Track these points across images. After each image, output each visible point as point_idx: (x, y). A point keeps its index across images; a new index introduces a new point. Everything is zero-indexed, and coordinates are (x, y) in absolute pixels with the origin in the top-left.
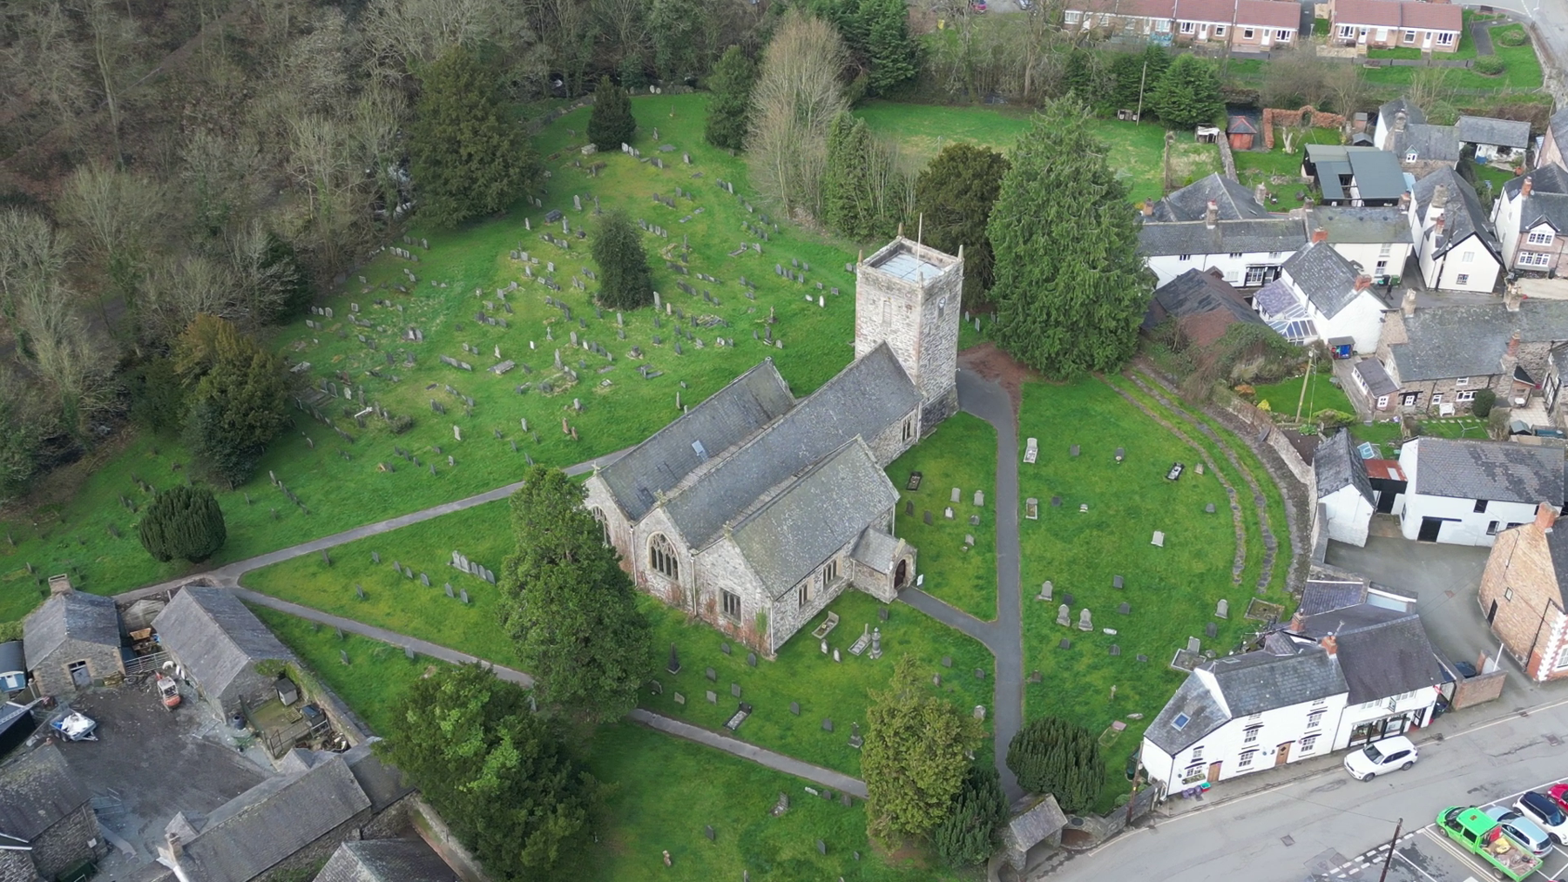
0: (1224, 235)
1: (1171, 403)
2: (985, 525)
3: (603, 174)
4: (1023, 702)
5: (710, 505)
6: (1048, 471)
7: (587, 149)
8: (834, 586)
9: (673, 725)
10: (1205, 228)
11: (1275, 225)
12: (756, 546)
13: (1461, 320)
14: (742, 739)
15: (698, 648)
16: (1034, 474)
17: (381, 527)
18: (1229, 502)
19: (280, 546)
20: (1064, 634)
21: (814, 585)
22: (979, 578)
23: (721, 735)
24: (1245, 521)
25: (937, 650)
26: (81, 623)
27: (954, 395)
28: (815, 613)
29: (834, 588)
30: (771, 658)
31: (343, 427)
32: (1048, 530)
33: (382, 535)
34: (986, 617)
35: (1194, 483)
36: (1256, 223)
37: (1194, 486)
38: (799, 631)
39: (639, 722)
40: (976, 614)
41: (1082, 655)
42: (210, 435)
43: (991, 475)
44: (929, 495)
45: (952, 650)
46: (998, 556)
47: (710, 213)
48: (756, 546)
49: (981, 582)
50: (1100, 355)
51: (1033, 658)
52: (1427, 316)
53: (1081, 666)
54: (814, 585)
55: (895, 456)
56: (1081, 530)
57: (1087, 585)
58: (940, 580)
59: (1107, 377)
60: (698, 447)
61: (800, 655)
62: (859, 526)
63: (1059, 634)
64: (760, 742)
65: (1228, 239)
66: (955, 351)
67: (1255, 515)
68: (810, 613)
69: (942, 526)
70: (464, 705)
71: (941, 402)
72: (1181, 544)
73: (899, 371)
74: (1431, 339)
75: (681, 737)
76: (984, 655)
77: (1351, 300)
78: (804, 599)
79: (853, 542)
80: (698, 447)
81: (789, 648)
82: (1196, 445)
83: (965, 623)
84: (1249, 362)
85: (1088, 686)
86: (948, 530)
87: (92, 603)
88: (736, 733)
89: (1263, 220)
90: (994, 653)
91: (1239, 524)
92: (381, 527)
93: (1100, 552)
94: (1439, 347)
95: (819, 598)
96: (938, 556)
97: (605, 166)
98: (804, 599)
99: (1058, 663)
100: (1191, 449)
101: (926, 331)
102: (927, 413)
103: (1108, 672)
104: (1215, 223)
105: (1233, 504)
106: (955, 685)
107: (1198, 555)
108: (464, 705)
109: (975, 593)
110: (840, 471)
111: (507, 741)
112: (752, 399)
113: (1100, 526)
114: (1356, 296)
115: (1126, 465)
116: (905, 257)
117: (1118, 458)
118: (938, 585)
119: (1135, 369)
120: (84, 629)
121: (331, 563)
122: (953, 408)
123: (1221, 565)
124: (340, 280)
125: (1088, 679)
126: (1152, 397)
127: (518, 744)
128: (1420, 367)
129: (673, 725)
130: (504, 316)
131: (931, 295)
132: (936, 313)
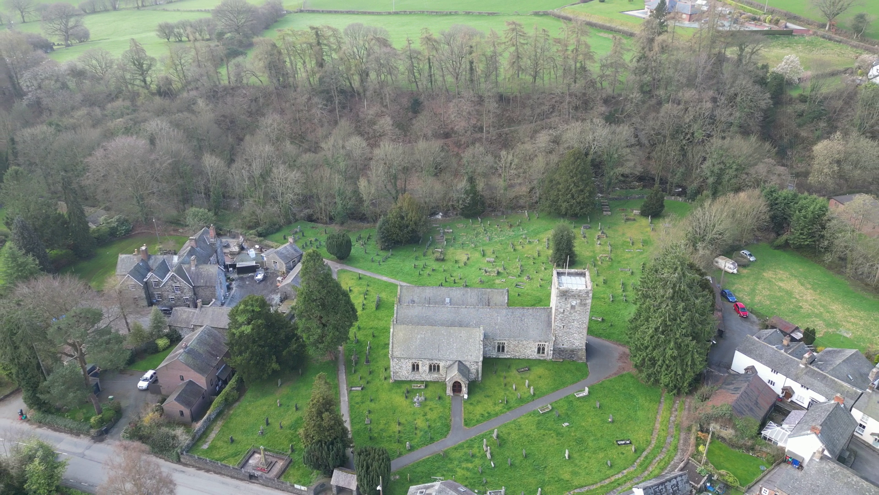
0: (806, 374)
1: (674, 422)
2: (521, 400)
3: (628, 223)
4: (427, 457)
5: (416, 316)
6: (578, 403)
7: (636, 212)
8: (436, 376)
9: (343, 377)
10: (798, 365)
11: (842, 386)
12: (401, 334)
13: (847, 483)
14: (348, 394)
15: (382, 363)
16: (570, 401)
17: (385, 278)
18: (625, 469)
19: (360, 268)
20: (479, 452)
21: (424, 368)
22: (488, 413)
23: (347, 389)
24: (616, 481)
25: (435, 420)
26: (284, 252)
27: (584, 353)
28: (423, 380)
29: (434, 376)
30: (391, 381)
31: (430, 251)
32: (539, 420)
33: (381, 280)
34: (466, 425)
35: (624, 452)
36: (831, 379)
37: (623, 454)
38: (411, 381)
39: (338, 368)
40: (465, 421)
41: (472, 462)
42: (381, 228)
43: (556, 389)
44: (522, 378)
45: (439, 424)
46: (508, 413)
47: (641, 253)
48: (401, 334)
49: (487, 415)
50: (664, 380)
51: (456, 449)
52: (827, 467)
53: (464, 465)
54: (424, 368)
55: (530, 357)
56: (550, 430)
57: (517, 446)
58: (475, 403)
59: (665, 394)
60: (448, 300)
61: (400, 387)
62: (455, 357)
63: (478, 450)
64: (351, 399)
65: (806, 378)
66: (585, 332)
67: (625, 482)
68: (417, 377)
69: (508, 390)
70: (246, 306)
71: (572, 351)
72: (576, 465)
73: (549, 324)
74: (818, 480)
75: (338, 381)
76: (444, 434)
77: (804, 435)
78: (415, 368)
79: (449, 363)
80: (448, 300)
81: (399, 383)
82: (654, 442)
83: (458, 420)
84: (724, 426)
85: (456, 472)
86: (507, 392)
87: (295, 250)
88: (350, 391)
89: (836, 380)
90: (448, 436)
91: (613, 479)
92: (385, 278)
93: (542, 441)
94: (818, 486)
95: (424, 374)
96: (488, 396)
97: (634, 220)
98: (415, 368)
99: (460, 457)
100: (649, 443)
101: (562, 310)
102: (558, 351)
103: (468, 474)
104: (805, 365)
105: (625, 471)
106: (420, 434)
107: (574, 473)
108: (246, 306)
109: (478, 416)
110: (463, 333)
111: (250, 326)
112: (487, 299)
113: (558, 434)
114: (808, 434)
115: (610, 425)
116: (583, 279)
117: (610, 420)
118: (471, 404)
119: (684, 399)
120: (282, 253)
121: (360, 278)
122: (581, 359)
123: (576, 483)
124: (500, 214)
125: (458, 469)
126: (671, 413)
127: (253, 329)
128: (794, 487)
129: (343, 377)
130: (519, 248)
131: (564, 295)
132: (569, 306)
